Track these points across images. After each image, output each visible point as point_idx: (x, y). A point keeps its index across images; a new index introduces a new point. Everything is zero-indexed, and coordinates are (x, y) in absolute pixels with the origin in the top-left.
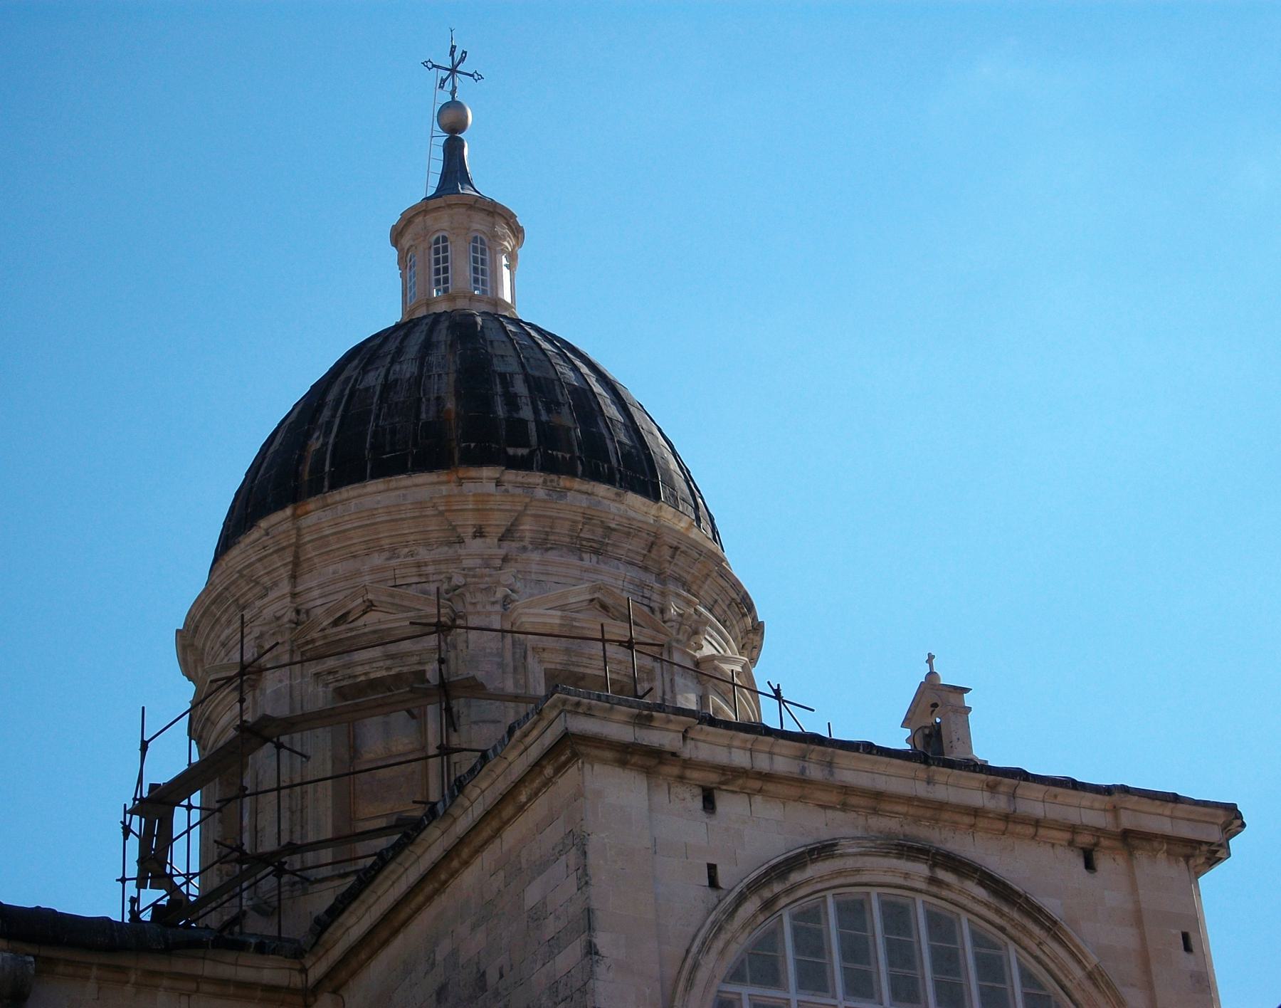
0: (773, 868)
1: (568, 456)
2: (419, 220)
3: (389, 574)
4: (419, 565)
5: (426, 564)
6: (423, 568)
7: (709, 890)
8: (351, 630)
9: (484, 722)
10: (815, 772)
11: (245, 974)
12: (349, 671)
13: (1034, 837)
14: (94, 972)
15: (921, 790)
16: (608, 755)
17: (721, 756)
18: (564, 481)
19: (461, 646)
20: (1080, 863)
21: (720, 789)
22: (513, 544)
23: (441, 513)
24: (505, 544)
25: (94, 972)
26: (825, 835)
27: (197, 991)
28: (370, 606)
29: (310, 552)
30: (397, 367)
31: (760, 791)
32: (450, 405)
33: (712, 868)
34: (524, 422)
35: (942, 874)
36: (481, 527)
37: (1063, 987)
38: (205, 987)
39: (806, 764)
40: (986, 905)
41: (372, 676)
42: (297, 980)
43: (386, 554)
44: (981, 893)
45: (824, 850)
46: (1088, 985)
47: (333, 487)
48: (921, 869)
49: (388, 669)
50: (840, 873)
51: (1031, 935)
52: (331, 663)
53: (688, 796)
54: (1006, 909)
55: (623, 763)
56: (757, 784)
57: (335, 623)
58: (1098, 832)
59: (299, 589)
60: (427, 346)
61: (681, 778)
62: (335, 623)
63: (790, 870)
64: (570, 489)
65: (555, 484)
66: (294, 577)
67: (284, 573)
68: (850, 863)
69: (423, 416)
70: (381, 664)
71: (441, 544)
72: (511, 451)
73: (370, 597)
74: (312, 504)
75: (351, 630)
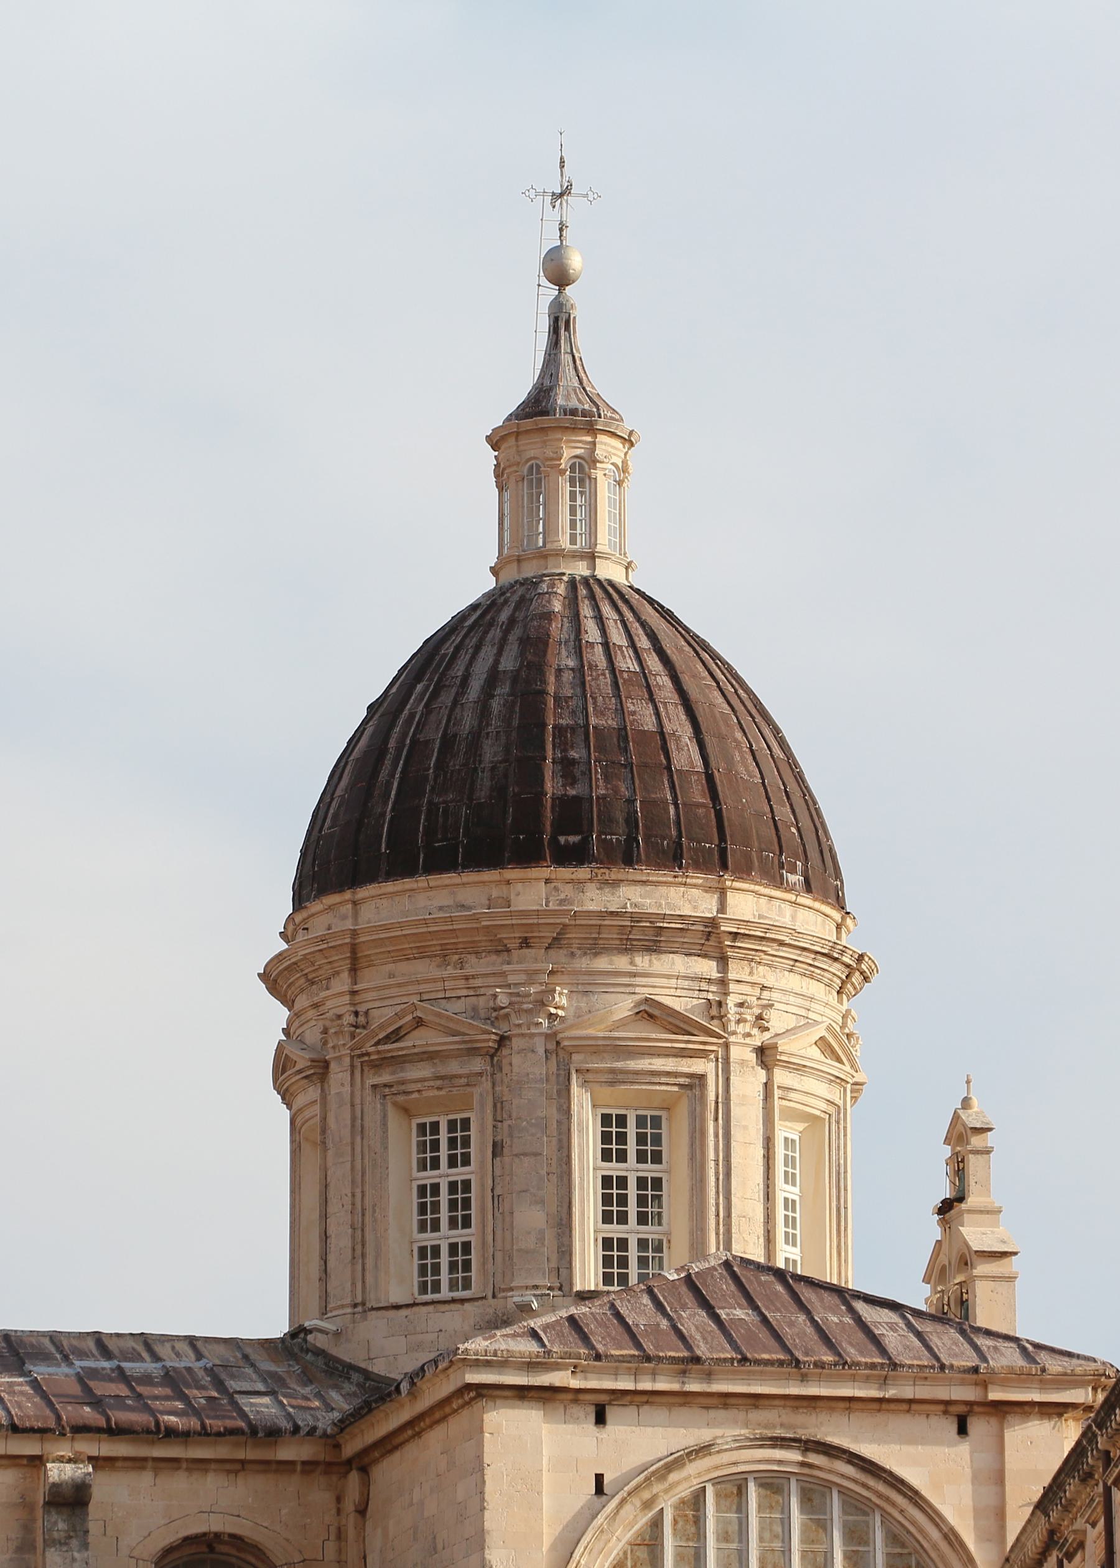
0: (653, 1473)
2: (512, 441)
3: (440, 986)
6: (471, 981)
7: (595, 1497)
8: (402, 1049)
9: (525, 1154)
12: (403, 1088)
13: (908, 1411)
18: (615, 874)
19: (506, 1069)
20: (954, 1427)
21: (610, 1404)
27: (243, 1469)
28: (419, 1023)
31: (647, 1402)
33: (599, 1478)
35: (814, 1459)
36: (526, 938)
37: (922, 1546)
40: (855, 1481)
44: (850, 1470)
45: (704, 1450)
46: (943, 1546)
48: (795, 1456)
51: (894, 1504)
52: (386, 1077)
53: (582, 1415)
54: (871, 1482)
55: (522, 1398)
56: (645, 1398)
57: (387, 1039)
58: (969, 1404)
59: (356, 988)
61: (576, 1401)
62: (387, 1039)
63: (670, 1472)
65: (607, 877)
66: (354, 970)
67: (346, 965)
68: (726, 1458)
70: (432, 1083)
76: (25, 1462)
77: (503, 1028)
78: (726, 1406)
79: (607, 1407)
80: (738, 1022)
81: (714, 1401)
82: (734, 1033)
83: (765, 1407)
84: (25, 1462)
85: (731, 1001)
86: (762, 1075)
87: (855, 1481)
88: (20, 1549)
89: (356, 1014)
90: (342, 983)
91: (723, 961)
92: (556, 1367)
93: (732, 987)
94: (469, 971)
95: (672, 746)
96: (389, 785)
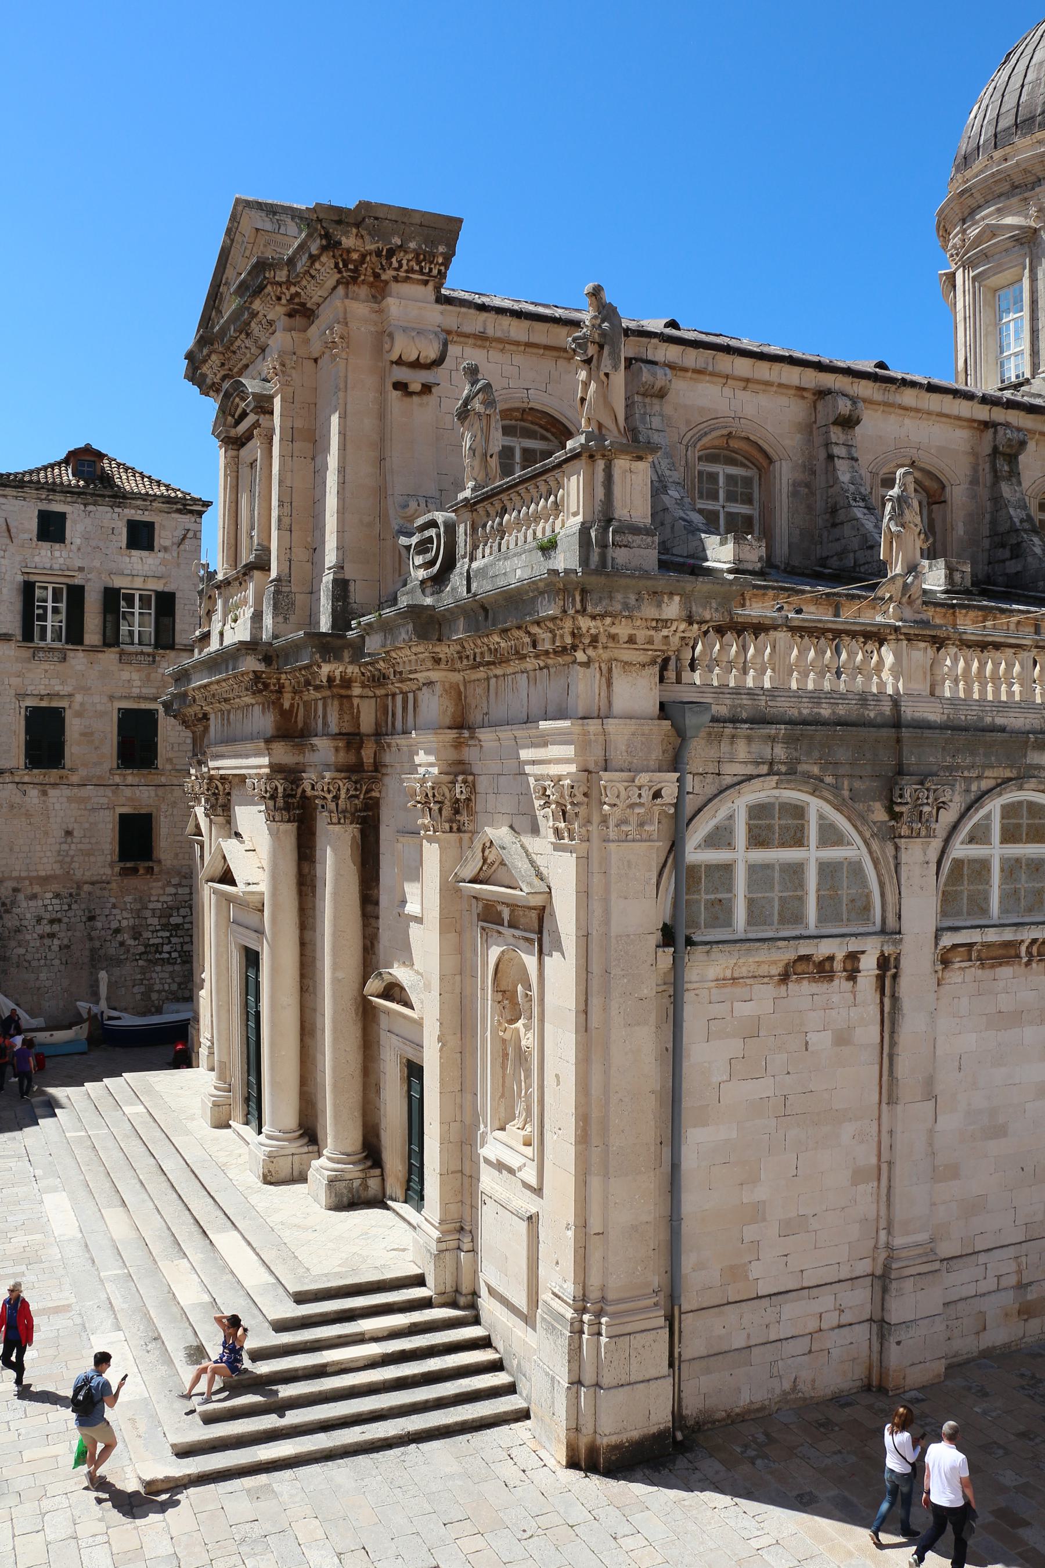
76: (976, 425)
84: (976, 425)
88: (971, 483)
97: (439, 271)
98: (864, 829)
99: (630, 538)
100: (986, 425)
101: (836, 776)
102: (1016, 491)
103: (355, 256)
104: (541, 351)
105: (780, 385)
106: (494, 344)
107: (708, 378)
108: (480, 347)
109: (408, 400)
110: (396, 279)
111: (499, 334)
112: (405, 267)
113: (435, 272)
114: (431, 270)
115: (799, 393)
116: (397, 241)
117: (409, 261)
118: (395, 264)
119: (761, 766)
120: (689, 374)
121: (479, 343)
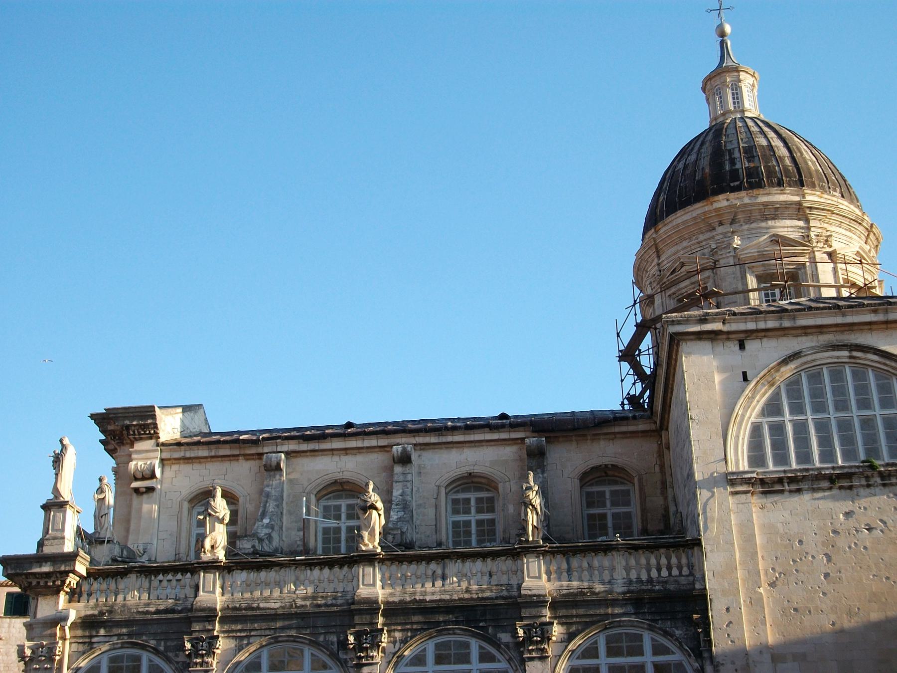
1: (757, 180)
2: (709, 83)
3: (689, 249)
4: (699, 243)
5: (702, 242)
10: (787, 324)
11: (631, 428)
12: (679, 292)
14: (574, 438)
15: (839, 320)
16: (692, 337)
17: (742, 327)
22: (737, 225)
23: (703, 220)
24: (733, 226)
25: (574, 438)
26: (797, 348)
27: (615, 438)
29: (661, 246)
30: (689, 158)
31: (765, 336)
32: (707, 171)
33: (745, 374)
34: (738, 170)
35: (855, 354)
36: (721, 221)
38: (618, 436)
39: (783, 322)
40: (879, 362)
41: (689, 292)
42: (653, 427)
43: (687, 241)
47: (667, 216)
48: (846, 353)
49: (694, 288)
50: (805, 363)
52: (673, 290)
53: (732, 345)
54: (888, 362)
55: (700, 339)
56: (763, 334)
57: (672, 274)
60: (703, 143)
61: (728, 339)
62: (672, 274)
64: (759, 195)
66: (659, 257)
67: (655, 255)
68: (809, 358)
69: (697, 178)
70: (690, 287)
71: (707, 231)
72: (732, 185)
73: (682, 260)
74: (660, 225)
75: (676, 276)
77: (716, 258)
78: (806, 334)
79: (745, 341)
80: (817, 242)
81: (799, 331)
82: (816, 247)
83: (826, 333)
84: (520, 441)
85: (812, 235)
86: (832, 265)
87: (879, 362)
89: (660, 271)
90: (656, 260)
91: (807, 221)
92: (714, 321)
93: (812, 229)
94: (699, 240)
95: (776, 149)
96: (666, 188)
97: (154, 431)
98: (171, 665)
99: (52, 541)
100: (523, 439)
101: (157, 640)
102: (539, 477)
103: (118, 432)
104: (220, 459)
105: (368, 448)
106: (194, 461)
107: (320, 453)
108: (188, 463)
109: (141, 497)
110: (136, 440)
111: (192, 455)
112: (136, 432)
113: (152, 432)
114: (150, 431)
115: (382, 449)
116: (127, 422)
117: (138, 430)
118: (131, 433)
119: (114, 637)
120: (308, 454)
121: (186, 461)
